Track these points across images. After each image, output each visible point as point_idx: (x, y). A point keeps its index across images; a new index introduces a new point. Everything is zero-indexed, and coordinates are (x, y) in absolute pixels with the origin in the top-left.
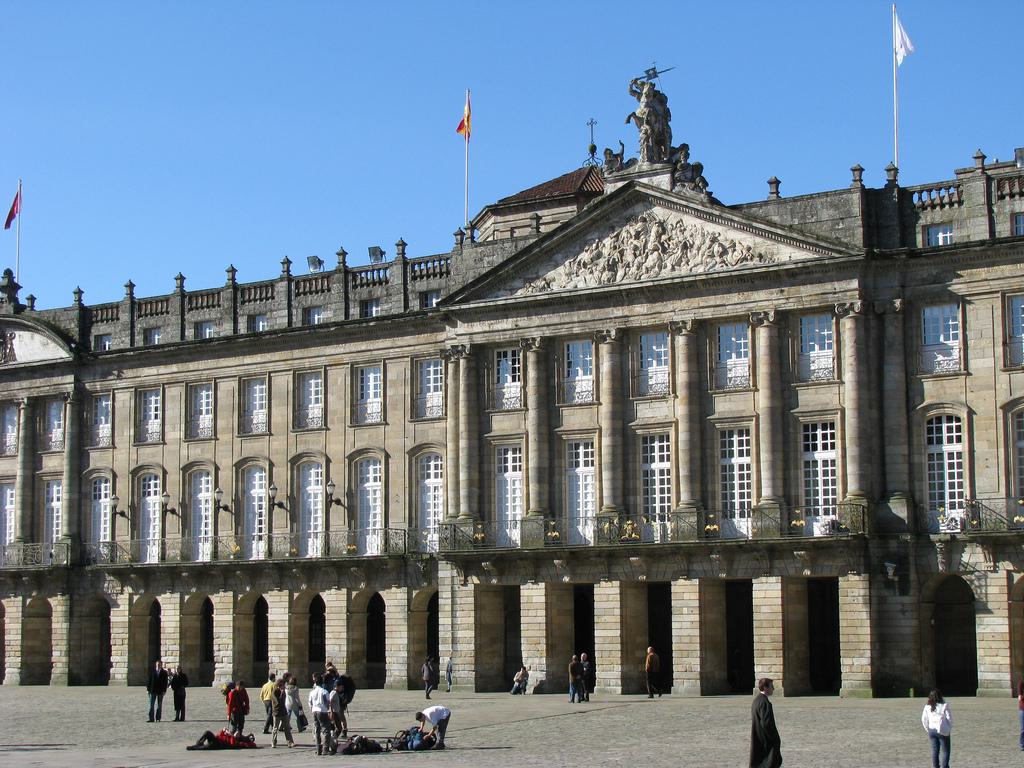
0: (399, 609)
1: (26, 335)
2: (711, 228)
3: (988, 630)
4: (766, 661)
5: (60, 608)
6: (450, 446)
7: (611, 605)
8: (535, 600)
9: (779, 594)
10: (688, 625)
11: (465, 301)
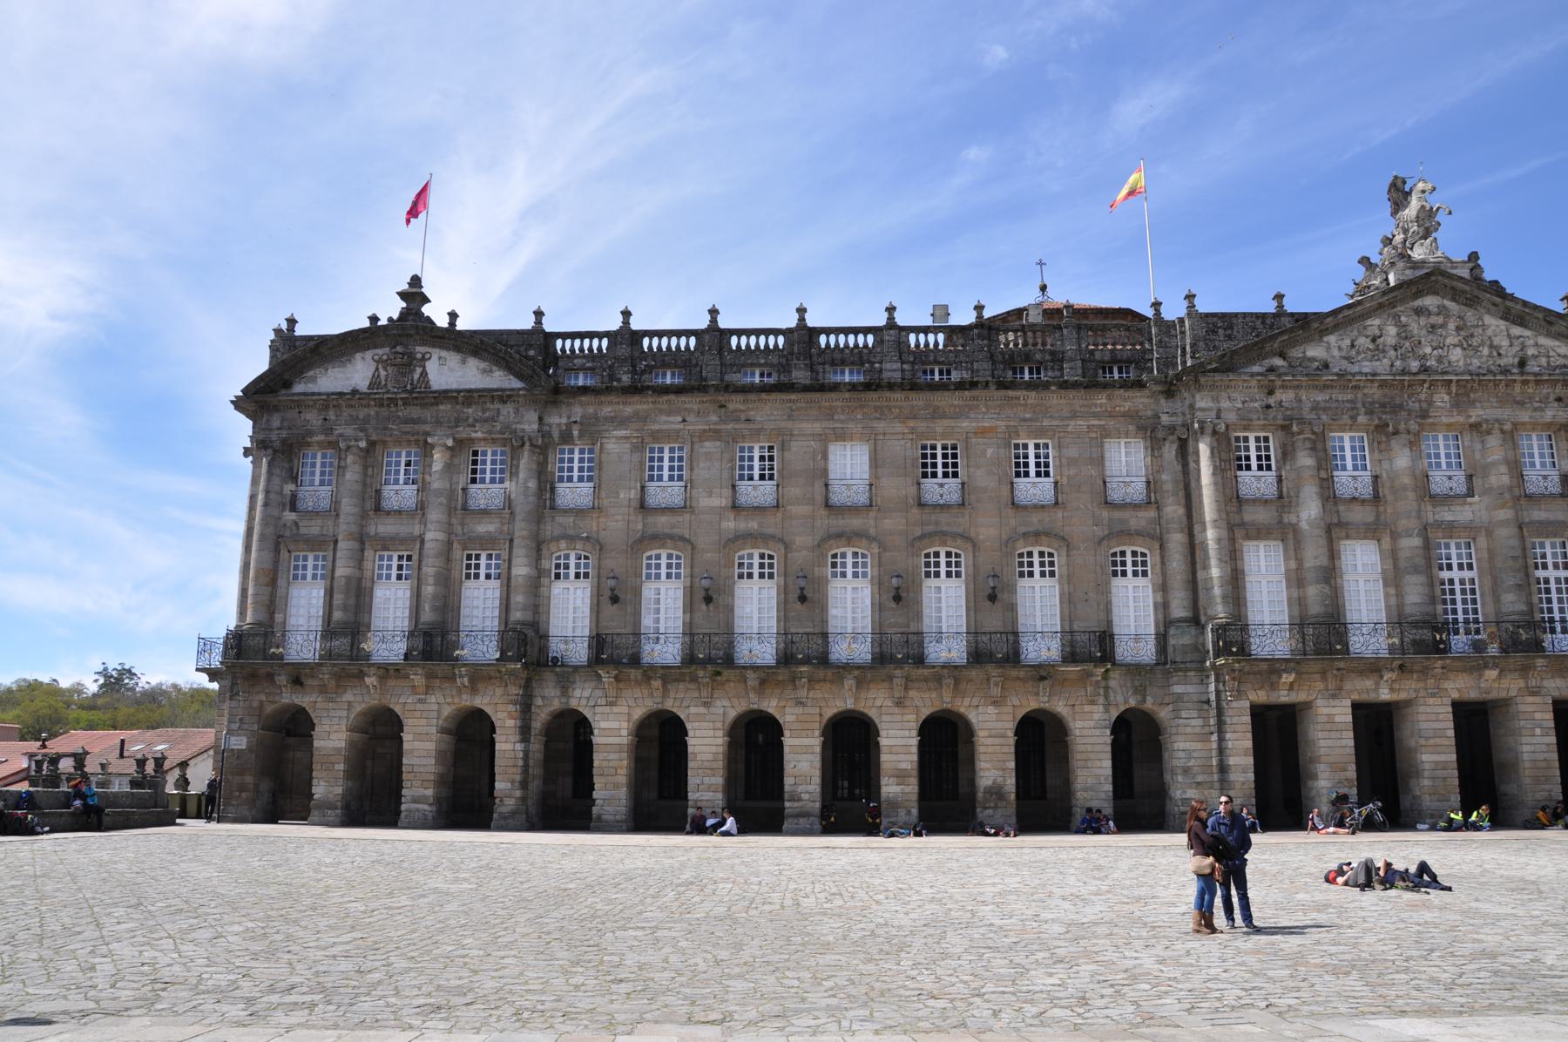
0: (1097, 732)
1: (453, 358)
2: (1517, 331)
5: (511, 723)
6: (1176, 540)
7: (1441, 725)
8: (1337, 719)
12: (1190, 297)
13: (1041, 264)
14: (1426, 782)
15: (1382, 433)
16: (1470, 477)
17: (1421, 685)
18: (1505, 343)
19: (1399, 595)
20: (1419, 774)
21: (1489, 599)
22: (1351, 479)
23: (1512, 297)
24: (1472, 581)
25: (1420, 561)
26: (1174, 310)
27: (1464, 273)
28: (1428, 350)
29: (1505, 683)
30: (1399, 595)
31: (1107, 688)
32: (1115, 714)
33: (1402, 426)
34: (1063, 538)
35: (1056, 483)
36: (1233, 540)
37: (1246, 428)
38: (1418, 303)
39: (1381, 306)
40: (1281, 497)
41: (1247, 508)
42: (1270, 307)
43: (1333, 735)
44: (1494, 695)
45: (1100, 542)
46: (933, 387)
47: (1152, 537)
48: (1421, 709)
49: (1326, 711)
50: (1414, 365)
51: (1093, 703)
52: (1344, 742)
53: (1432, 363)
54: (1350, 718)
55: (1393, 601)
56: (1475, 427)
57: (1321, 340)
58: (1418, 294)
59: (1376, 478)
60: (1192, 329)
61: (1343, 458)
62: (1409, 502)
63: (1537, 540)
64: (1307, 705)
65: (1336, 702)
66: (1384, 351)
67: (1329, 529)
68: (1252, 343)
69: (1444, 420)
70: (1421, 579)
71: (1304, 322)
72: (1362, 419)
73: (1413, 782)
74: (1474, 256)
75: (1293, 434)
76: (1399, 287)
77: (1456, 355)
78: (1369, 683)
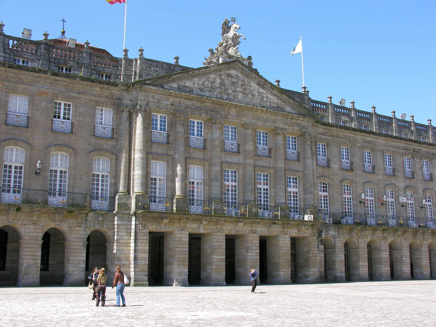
2: (261, 90)
3: (339, 259)
4: (284, 270)
7: (221, 244)
8: (183, 239)
9: (290, 242)
10: (255, 254)
11: (149, 84)
12: (141, 50)
13: (64, 21)
14: (214, 267)
15: (211, 122)
16: (239, 145)
17: (215, 227)
18: (257, 94)
19: (210, 190)
20: (211, 264)
21: (241, 194)
22: (196, 140)
23: (261, 77)
24: (235, 187)
25: (219, 177)
26: (133, 55)
27: (246, 63)
28: (230, 92)
29: (245, 227)
30: (210, 190)
31: (86, 220)
32: (89, 232)
33: (218, 121)
34: (73, 149)
35: (72, 124)
36: (147, 159)
37: (157, 112)
38: (228, 72)
39: (216, 70)
40: (168, 143)
41: (154, 146)
42: (173, 62)
43: (180, 246)
44: (240, 233)
45: (90, 152)
46: (19, 68)
47: (113, 153)
48: (214, 237)
49: (179, 236)
50: (225, 97)
51: (80, 226)
52: (185, 249)
53: (231, 97)
54: (187, 239)
55: (207, 192)
56: (243, 125)
57: (191, 80)
58: (229, 68)
59: (205, 140)
60: (140, 64)
61: (194, 130)
62: (217, 151)
63: (259, 173)
64: (171, 233)
65: (183, 232)
66: (214, 89)
67: (186, 158)
68: (166, 74)
69: (234, 121)
70: (219, 184)
71: (186, 70)
72: (203, 115)
73: (208, 267)
74: (250, 58)
75: (176, 117)
76: (223, 64)
77: (240, 96)
78: (196, 226)
